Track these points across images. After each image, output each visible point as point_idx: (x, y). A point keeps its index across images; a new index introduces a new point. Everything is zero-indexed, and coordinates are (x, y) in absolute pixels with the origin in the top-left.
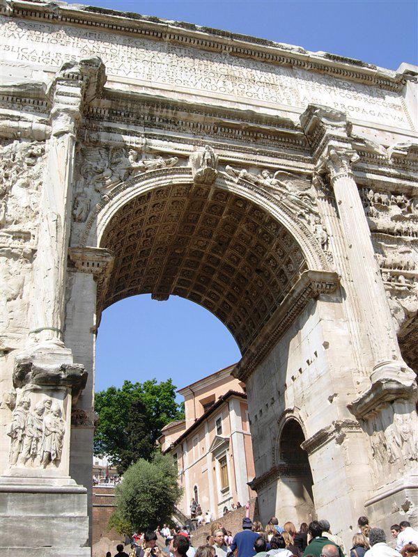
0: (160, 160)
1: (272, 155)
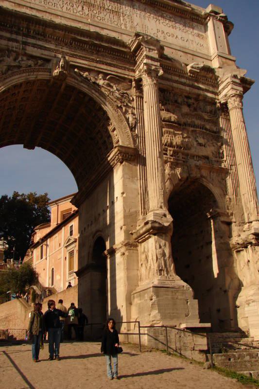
0: (30, 62)
1: (107, 64)
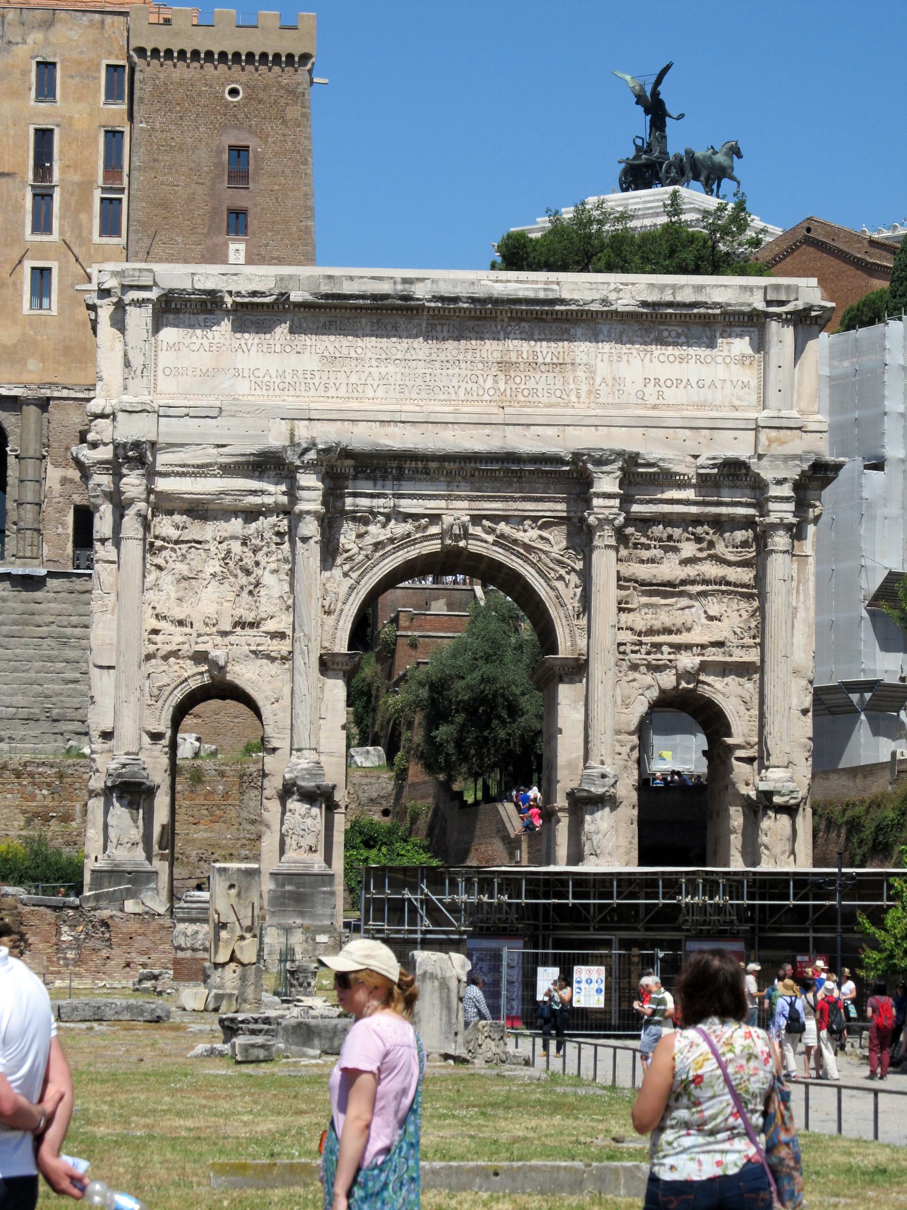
0: (408, 527)
